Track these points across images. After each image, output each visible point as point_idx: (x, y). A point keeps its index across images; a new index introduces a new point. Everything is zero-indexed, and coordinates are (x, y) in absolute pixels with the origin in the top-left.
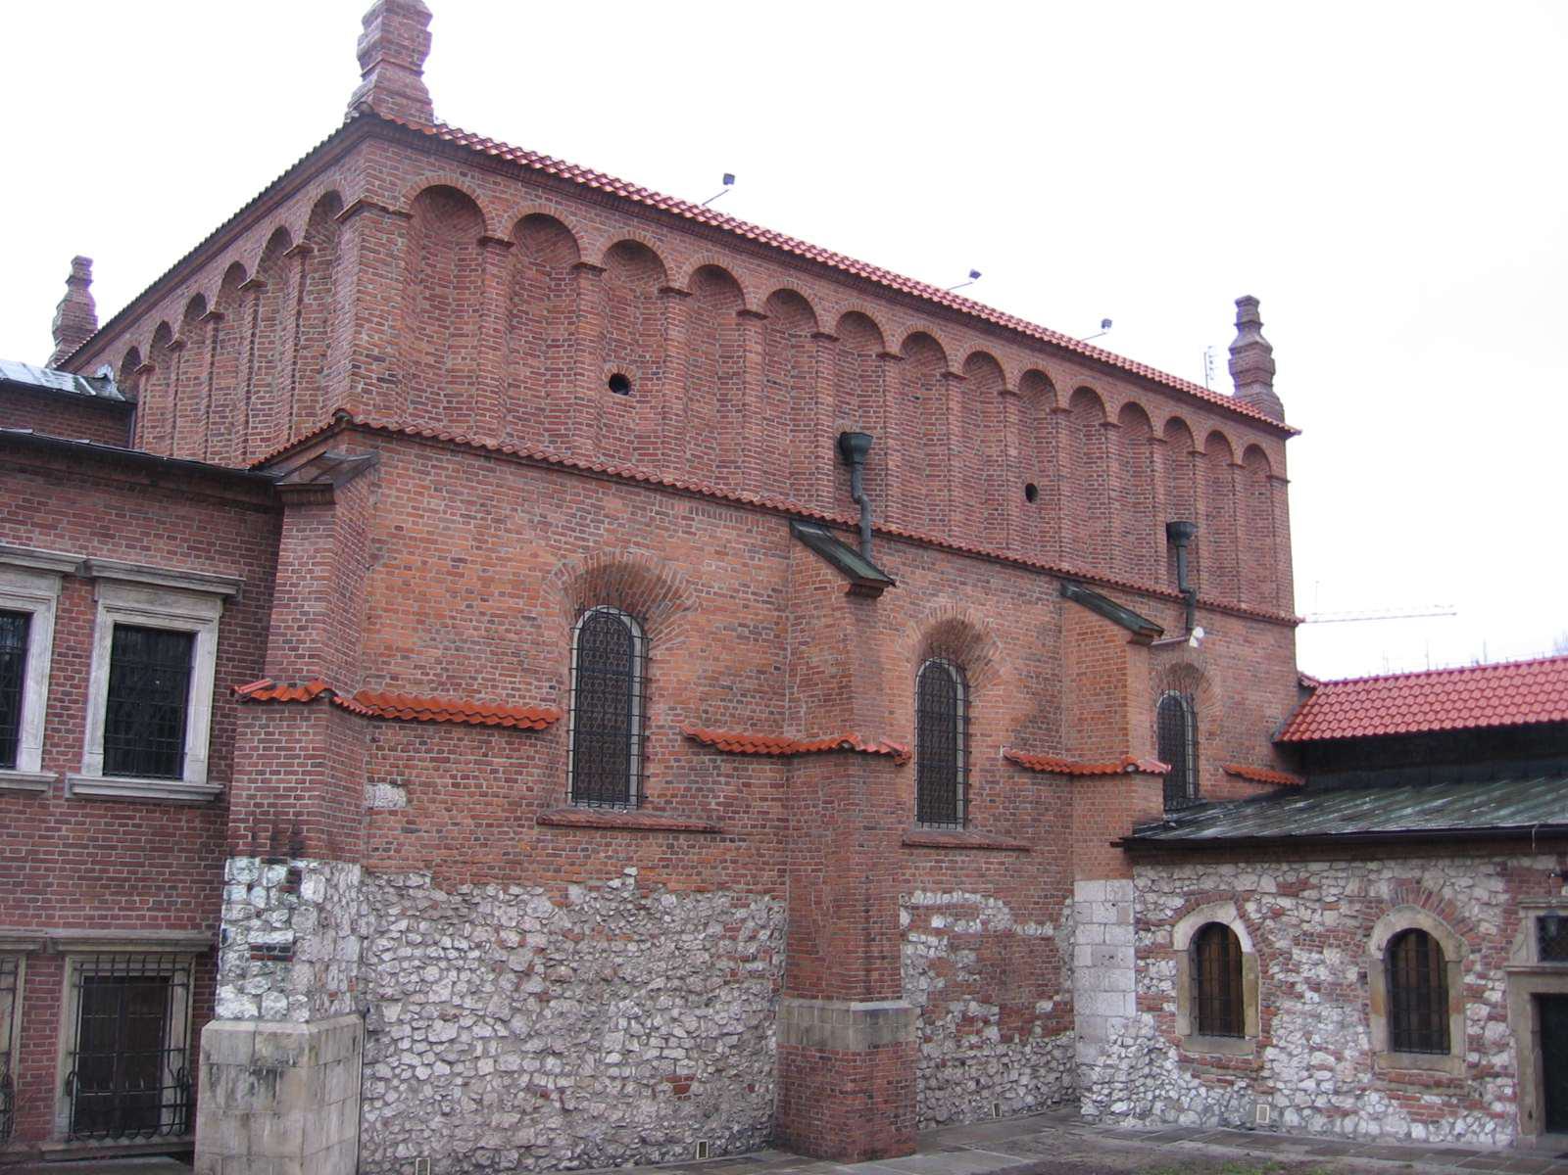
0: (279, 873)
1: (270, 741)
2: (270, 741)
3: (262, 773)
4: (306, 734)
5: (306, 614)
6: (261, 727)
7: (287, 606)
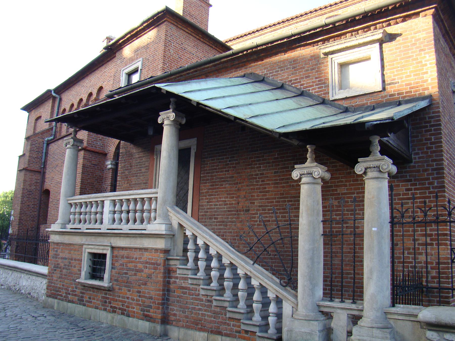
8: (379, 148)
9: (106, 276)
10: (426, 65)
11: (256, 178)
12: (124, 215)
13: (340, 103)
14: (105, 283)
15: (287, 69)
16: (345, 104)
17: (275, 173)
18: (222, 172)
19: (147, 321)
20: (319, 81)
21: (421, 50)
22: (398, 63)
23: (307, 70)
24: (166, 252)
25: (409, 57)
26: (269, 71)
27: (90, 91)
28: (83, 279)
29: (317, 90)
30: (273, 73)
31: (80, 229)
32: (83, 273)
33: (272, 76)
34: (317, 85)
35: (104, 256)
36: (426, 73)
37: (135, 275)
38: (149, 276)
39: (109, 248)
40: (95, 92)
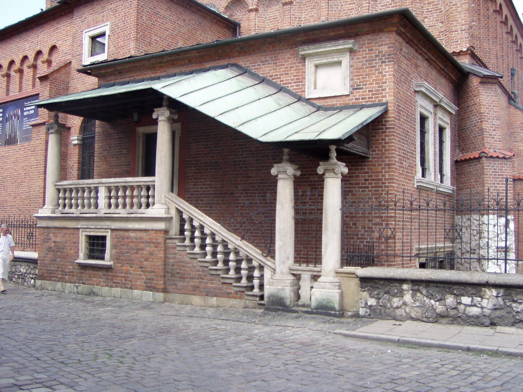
0: (503, 220)
1: (496, 172)
2: (496, 172)
3: (494, 184)
4: (506, 170)
5: (495, 125)
6: (492, 167)
7: (488, 121)
8: (336, 154)
9: (107, 255)
10: (385, 76)
11: (239, 164)
12: (120, 200)
13: (314, 102)
14: (107, 261)
15: (269, 64)
16: (318, 103)
17: (257, 160)
18: (207, 157)
19: (151, 291)
20: (297, 79)
21: (382, 62)
22: (364, 71)
23: (287, 68)
24: (166, 232)
25: (373, 67)
26: (251, 63)
27: (38, 49)
28: (82, 259)
29: (295, 87)
30: (255, 66)
32: (81, 255)
33: (254, 69)
34: (295, 82)
35: (104, 238)
36: (385, 83)
37: (137, 253)
38: (151, 254)
39: (109, 231)
40: (46, 51)
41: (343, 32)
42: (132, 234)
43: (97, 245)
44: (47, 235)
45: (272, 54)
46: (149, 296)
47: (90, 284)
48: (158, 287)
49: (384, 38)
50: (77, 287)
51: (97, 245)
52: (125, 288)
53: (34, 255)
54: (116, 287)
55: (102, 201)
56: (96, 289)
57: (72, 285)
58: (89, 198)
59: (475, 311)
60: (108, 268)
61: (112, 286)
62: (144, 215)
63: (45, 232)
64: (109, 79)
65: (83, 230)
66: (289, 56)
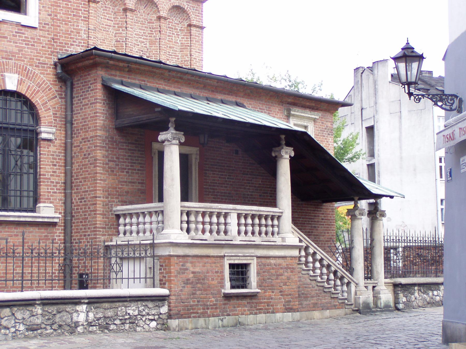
11: (248, 198)
12: (250, 228)
17: (260, 196)
18: (222, 187)
19: (289, 312)
21: (329, 134)
28: (228, 289)
31: (232, 241)
37: (277, 279)
38: (288, 278)
39: (255, 258)
41: (314, 105)
42: (273, 261)
43: (239, 272)
44: (182, 265)
45: (267, 105)
46: (289, 316)
47: (235, 315)
48: (295, 307)
49: (328, 117)
50: (222, 320)
51: (239, 272)
52: (268, 313)
53: (165, 292)
54: (260, 313)
55: (233, 227)
56: (242, 318)
57: (216, 319)
58: (218, 224)
59: (438, 298)
60: (253, 296)
61: (256, 314)
62: (231, 242)
63: (180, 262)
64: (113, 72)
65: (228, 258)
66: (277, 110)
